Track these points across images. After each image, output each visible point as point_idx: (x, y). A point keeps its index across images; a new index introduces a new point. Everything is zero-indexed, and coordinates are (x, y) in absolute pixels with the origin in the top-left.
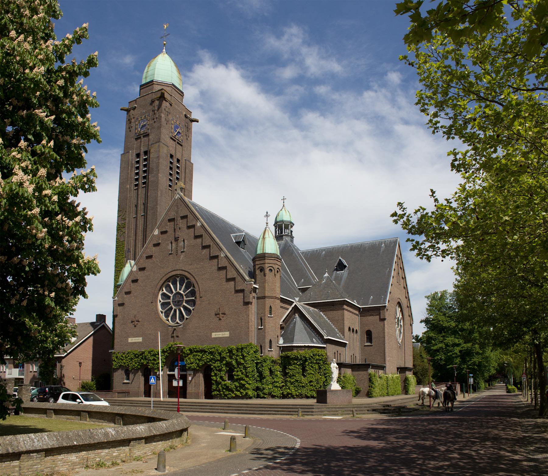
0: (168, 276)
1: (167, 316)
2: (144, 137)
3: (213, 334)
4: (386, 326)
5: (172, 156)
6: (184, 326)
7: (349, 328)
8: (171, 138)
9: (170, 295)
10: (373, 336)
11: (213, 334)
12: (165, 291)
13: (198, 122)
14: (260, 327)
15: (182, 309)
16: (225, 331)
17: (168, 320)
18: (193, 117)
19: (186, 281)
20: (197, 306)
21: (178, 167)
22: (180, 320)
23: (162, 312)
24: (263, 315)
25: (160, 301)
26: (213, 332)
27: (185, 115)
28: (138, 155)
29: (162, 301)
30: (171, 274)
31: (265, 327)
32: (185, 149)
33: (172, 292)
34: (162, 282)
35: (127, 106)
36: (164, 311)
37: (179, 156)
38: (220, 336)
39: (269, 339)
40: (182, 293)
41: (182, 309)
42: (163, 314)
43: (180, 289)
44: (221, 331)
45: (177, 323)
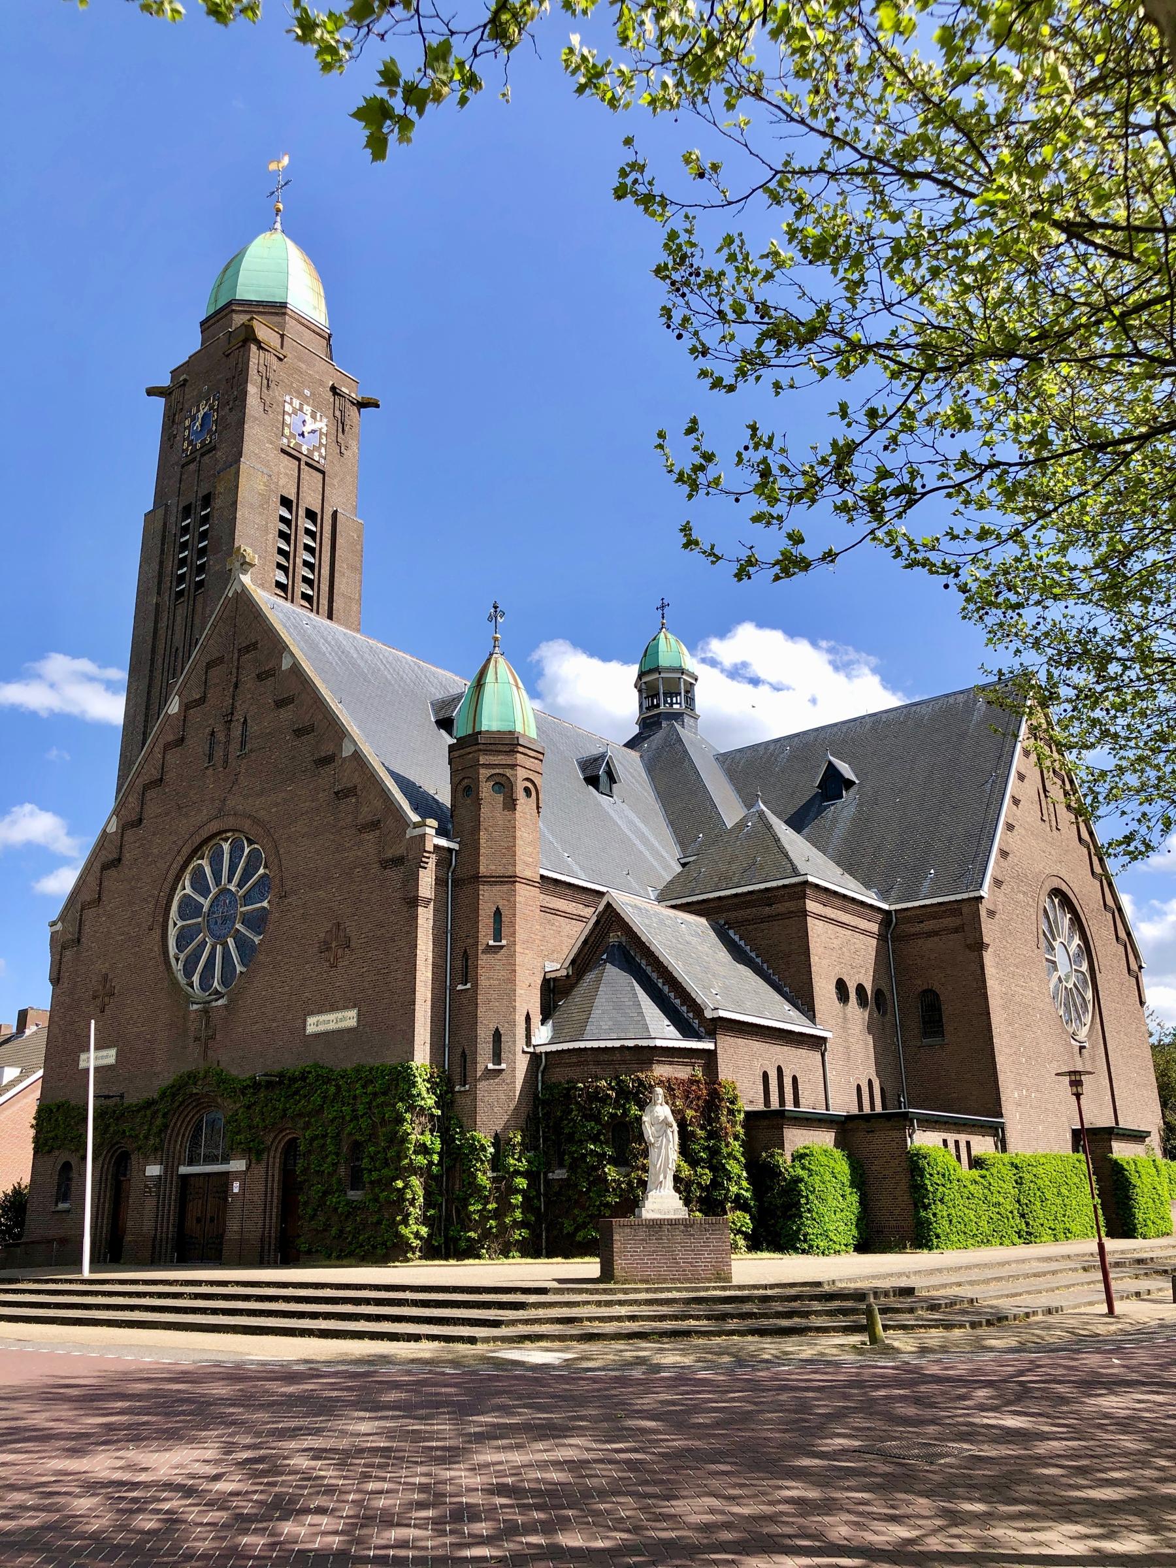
0: (198, 840)
1: (188, 974)
3: (311, 1020)
4: (990, 971)
5: (286, 502)
6: (230, 1001)
7: (841, 986)
8: (283, 451)
9: (201, 900)
10: (947, 1009)
11: (311, 1020)
12: (188, 890)
13: (377, 406)
14: (460, 987)
15: (230, 941)
16: (345, 1008)
17: (191, 985)
19: (247, 851)
20: (270, 927)
22: (224, 982)
23: (177, 960)
24: (470, 941)
25: (175, 924)
26: (312, 1013)
28: (187, 511)
29: (180, 924)
30: (205, 834)
31: (475, 985)
32: (335, 482)
33: (205, 892)
34: (180, 860)
35: (166, 381)
36: (182, 956)
37: (310, 500)
38: (332, 1026)
39: (492, 1027)
40: (233, 889)
41: (230, 941)
42: (180, 966)
43: (230, 881)
44: (333, 1008)
45: (217, 992)
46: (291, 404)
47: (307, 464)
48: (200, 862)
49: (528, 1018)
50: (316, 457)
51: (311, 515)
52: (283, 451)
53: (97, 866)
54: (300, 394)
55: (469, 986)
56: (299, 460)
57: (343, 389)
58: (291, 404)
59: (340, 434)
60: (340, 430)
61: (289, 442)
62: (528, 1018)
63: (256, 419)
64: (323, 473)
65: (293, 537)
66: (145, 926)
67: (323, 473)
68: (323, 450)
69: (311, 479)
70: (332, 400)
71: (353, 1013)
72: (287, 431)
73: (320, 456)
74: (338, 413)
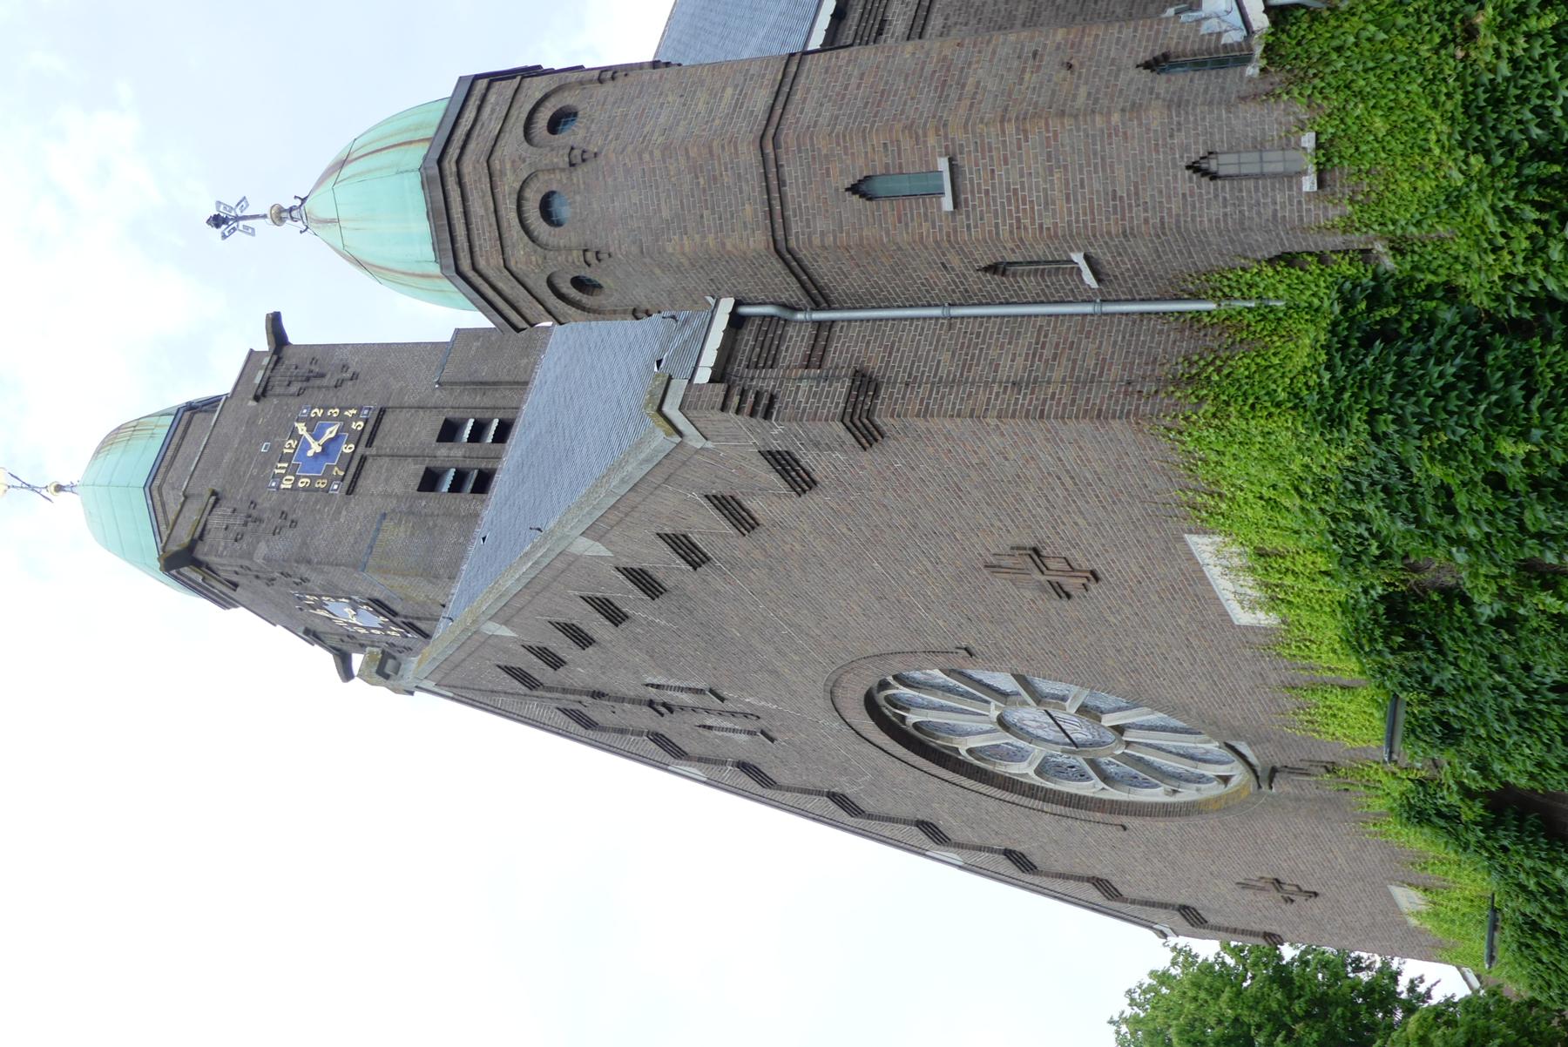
2: (395, 614)
5: (430, 481)
8: (350, 491)
14: (1089, 278)
16: (1191, 557)
18: (263, 344)
21: (477, 435)
24: (955, 261)
27: (257, 398)
39: (1186, 182)
46: (281, 476)
47: (369, 444)
48: (963, 752)
49: (1157, 64)
50: (358, 425)
51: (449, 432)
52: (350, 491)
53: (1028, 878)
54: (267, 462)
55: (1078, 257)
56: (363, 459)
57: (257, 381)
58: (281, 476)
59: (325, 382)
60: (318, 382)
61: (337, 477)
62: (1157, 64)
63: (304, 543)
64: (383, 411)
65: (483, 466)
66: (1121, 833)
67: (383, 411)
68: (349, 413)
69: (394, 434)
70: (275, 401)
71: (1203, 547)
72: (320, 484)
73: (356, 418)
74: (294, 388)
